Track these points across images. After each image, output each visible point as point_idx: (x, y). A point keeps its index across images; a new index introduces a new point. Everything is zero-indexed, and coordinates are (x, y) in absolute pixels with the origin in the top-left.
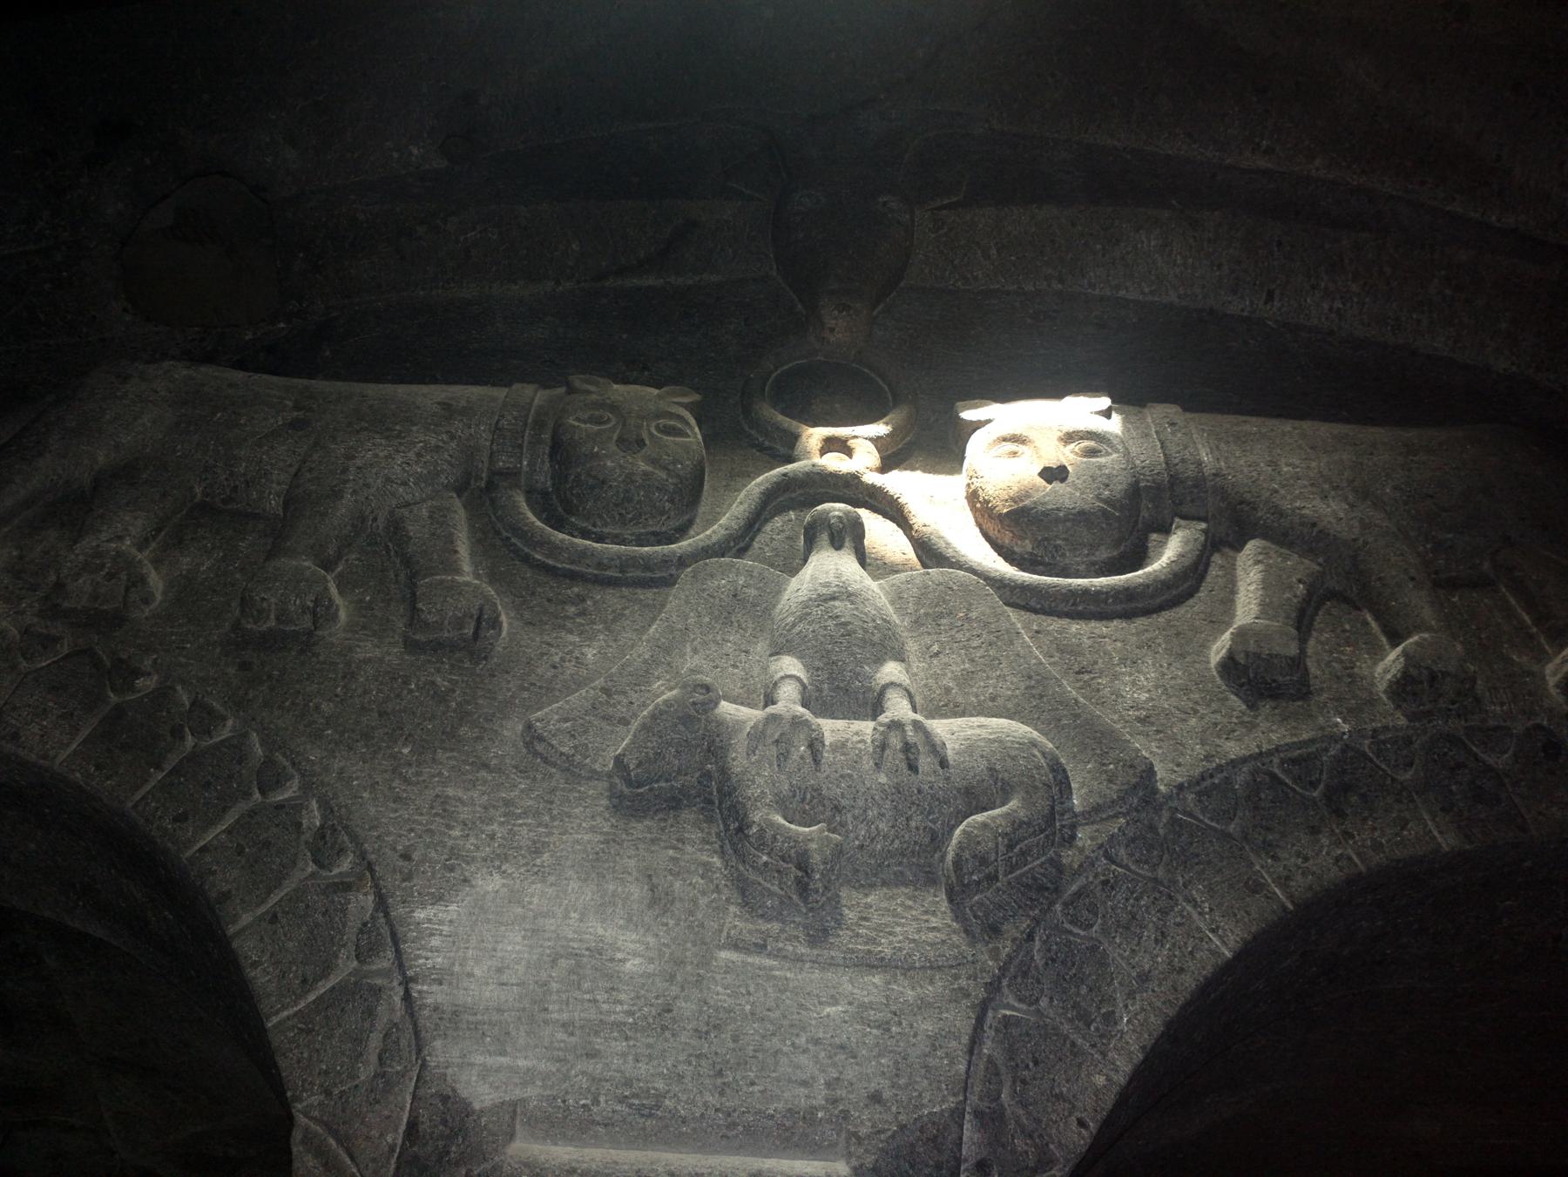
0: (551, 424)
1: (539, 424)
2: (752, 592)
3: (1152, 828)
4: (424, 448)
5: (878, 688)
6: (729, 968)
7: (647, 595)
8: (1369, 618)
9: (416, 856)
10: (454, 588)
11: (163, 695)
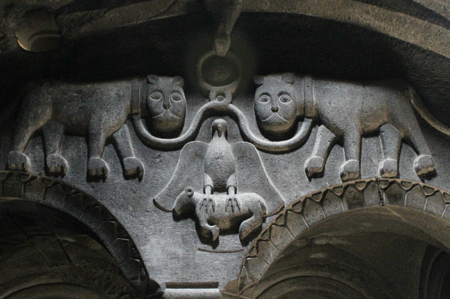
0: (145, 97)
2: (200, 152)
4: (117, 114)
5: (227, 187)
7: (174, 153)
8: (344, 150)
10: (132, 161)
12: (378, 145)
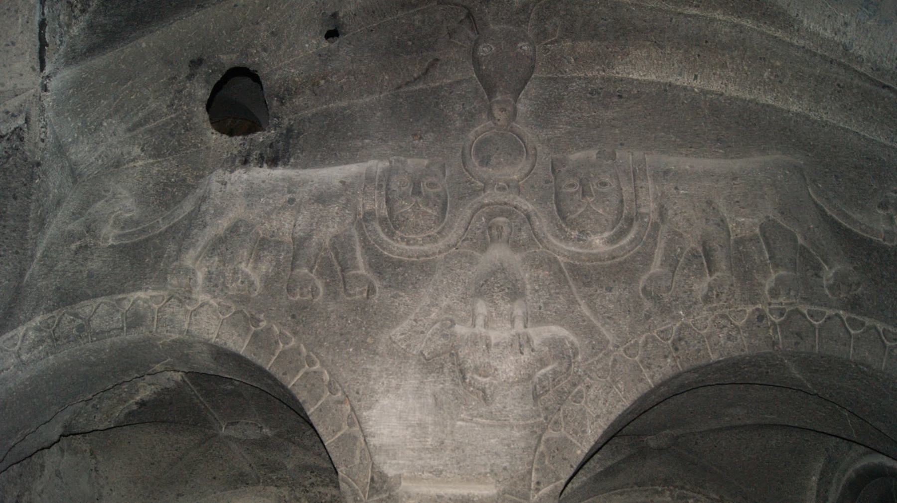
1: (380, 186)
3: (607, 365)
6: (461, 427)
9: (360, 392)
10: (357, 277)
11: (269, 330)
12: (761, 252)
